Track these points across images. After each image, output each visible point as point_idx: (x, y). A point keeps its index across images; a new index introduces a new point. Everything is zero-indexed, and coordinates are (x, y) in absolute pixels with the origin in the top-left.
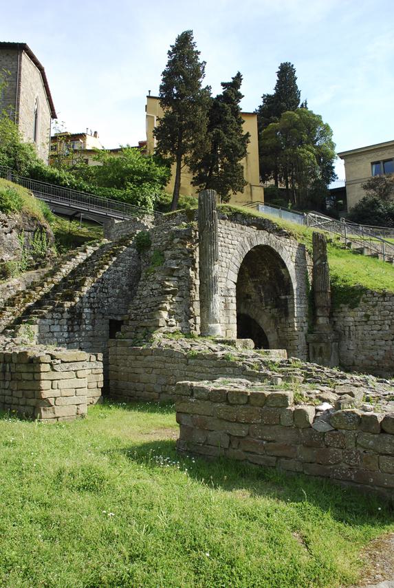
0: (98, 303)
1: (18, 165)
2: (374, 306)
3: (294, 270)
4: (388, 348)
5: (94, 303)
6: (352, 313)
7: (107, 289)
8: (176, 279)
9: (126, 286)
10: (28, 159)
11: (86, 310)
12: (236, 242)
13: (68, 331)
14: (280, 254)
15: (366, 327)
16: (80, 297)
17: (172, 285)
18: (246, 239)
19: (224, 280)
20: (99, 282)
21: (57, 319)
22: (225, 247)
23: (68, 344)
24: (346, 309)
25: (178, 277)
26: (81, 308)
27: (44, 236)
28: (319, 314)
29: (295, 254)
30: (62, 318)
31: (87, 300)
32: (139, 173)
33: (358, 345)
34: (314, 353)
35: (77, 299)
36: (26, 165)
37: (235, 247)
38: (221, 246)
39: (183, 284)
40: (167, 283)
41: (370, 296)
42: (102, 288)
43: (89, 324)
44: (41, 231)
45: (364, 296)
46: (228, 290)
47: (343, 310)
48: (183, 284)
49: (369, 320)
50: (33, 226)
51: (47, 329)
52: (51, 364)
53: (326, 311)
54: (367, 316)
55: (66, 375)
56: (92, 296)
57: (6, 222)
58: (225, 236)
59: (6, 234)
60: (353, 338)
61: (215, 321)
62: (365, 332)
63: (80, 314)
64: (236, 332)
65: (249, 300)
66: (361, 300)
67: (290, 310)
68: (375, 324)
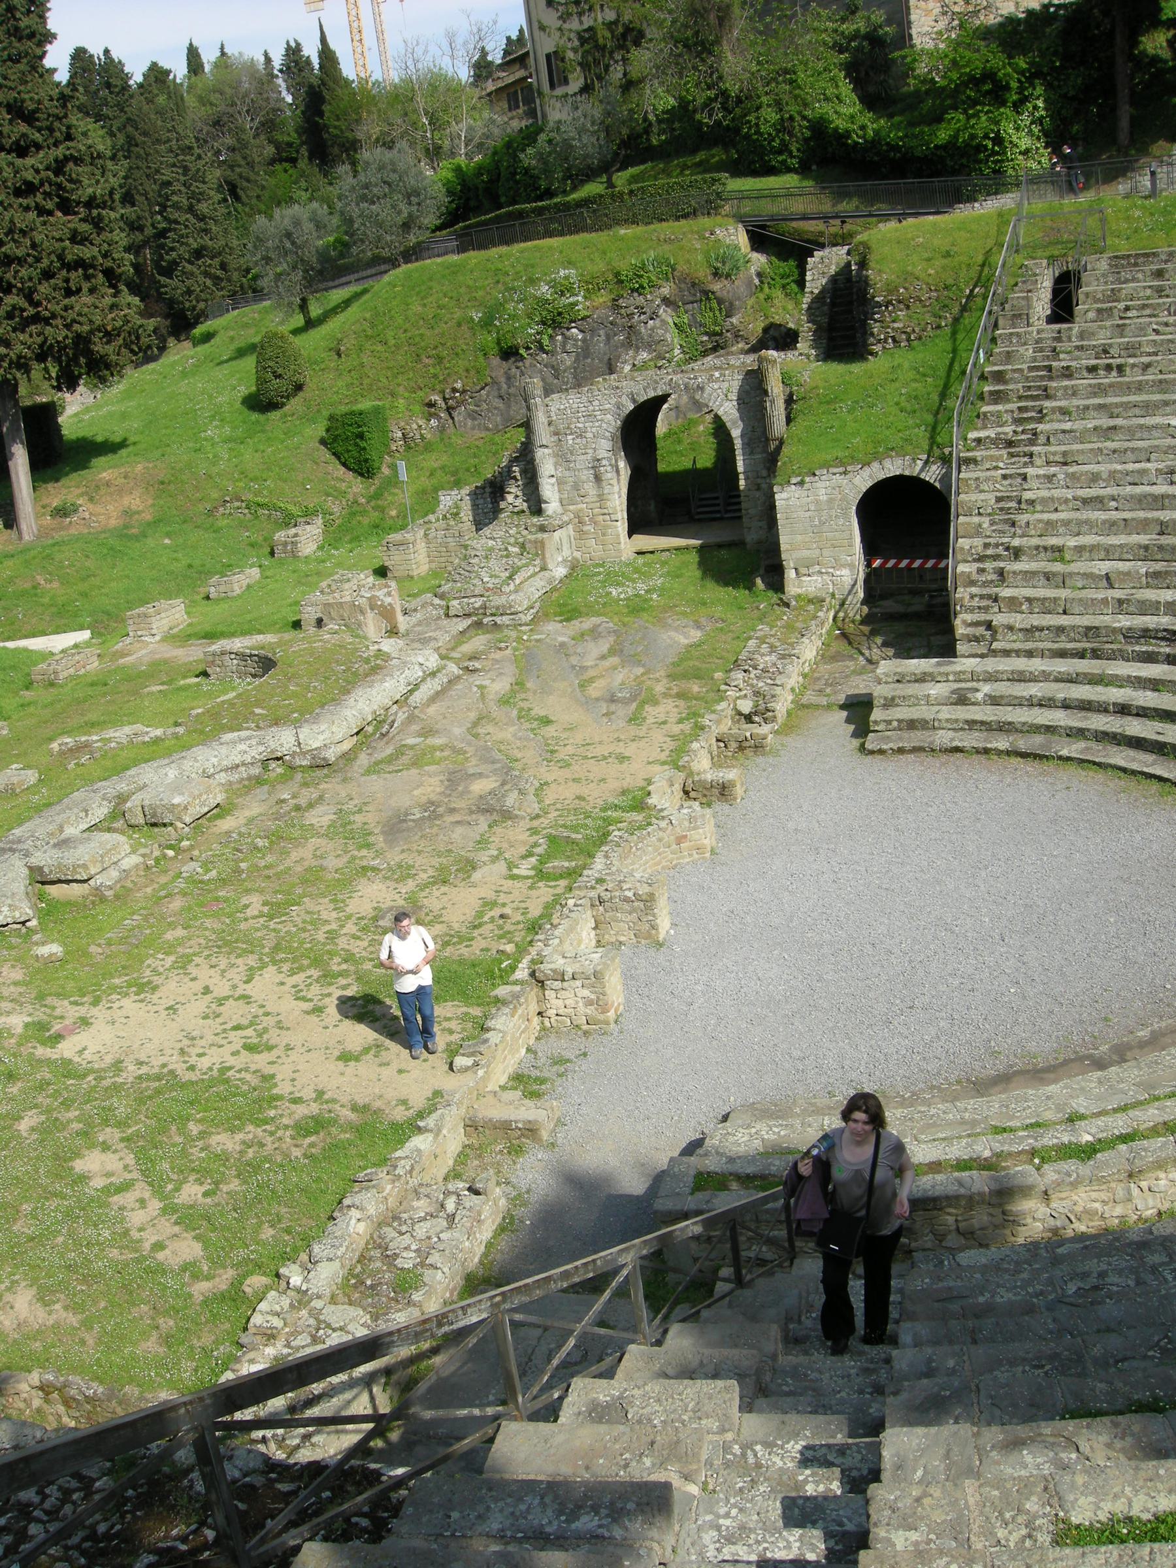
10: (806, 105)
27: (715, 305)
36: (804, 118)
44: (708, 299)
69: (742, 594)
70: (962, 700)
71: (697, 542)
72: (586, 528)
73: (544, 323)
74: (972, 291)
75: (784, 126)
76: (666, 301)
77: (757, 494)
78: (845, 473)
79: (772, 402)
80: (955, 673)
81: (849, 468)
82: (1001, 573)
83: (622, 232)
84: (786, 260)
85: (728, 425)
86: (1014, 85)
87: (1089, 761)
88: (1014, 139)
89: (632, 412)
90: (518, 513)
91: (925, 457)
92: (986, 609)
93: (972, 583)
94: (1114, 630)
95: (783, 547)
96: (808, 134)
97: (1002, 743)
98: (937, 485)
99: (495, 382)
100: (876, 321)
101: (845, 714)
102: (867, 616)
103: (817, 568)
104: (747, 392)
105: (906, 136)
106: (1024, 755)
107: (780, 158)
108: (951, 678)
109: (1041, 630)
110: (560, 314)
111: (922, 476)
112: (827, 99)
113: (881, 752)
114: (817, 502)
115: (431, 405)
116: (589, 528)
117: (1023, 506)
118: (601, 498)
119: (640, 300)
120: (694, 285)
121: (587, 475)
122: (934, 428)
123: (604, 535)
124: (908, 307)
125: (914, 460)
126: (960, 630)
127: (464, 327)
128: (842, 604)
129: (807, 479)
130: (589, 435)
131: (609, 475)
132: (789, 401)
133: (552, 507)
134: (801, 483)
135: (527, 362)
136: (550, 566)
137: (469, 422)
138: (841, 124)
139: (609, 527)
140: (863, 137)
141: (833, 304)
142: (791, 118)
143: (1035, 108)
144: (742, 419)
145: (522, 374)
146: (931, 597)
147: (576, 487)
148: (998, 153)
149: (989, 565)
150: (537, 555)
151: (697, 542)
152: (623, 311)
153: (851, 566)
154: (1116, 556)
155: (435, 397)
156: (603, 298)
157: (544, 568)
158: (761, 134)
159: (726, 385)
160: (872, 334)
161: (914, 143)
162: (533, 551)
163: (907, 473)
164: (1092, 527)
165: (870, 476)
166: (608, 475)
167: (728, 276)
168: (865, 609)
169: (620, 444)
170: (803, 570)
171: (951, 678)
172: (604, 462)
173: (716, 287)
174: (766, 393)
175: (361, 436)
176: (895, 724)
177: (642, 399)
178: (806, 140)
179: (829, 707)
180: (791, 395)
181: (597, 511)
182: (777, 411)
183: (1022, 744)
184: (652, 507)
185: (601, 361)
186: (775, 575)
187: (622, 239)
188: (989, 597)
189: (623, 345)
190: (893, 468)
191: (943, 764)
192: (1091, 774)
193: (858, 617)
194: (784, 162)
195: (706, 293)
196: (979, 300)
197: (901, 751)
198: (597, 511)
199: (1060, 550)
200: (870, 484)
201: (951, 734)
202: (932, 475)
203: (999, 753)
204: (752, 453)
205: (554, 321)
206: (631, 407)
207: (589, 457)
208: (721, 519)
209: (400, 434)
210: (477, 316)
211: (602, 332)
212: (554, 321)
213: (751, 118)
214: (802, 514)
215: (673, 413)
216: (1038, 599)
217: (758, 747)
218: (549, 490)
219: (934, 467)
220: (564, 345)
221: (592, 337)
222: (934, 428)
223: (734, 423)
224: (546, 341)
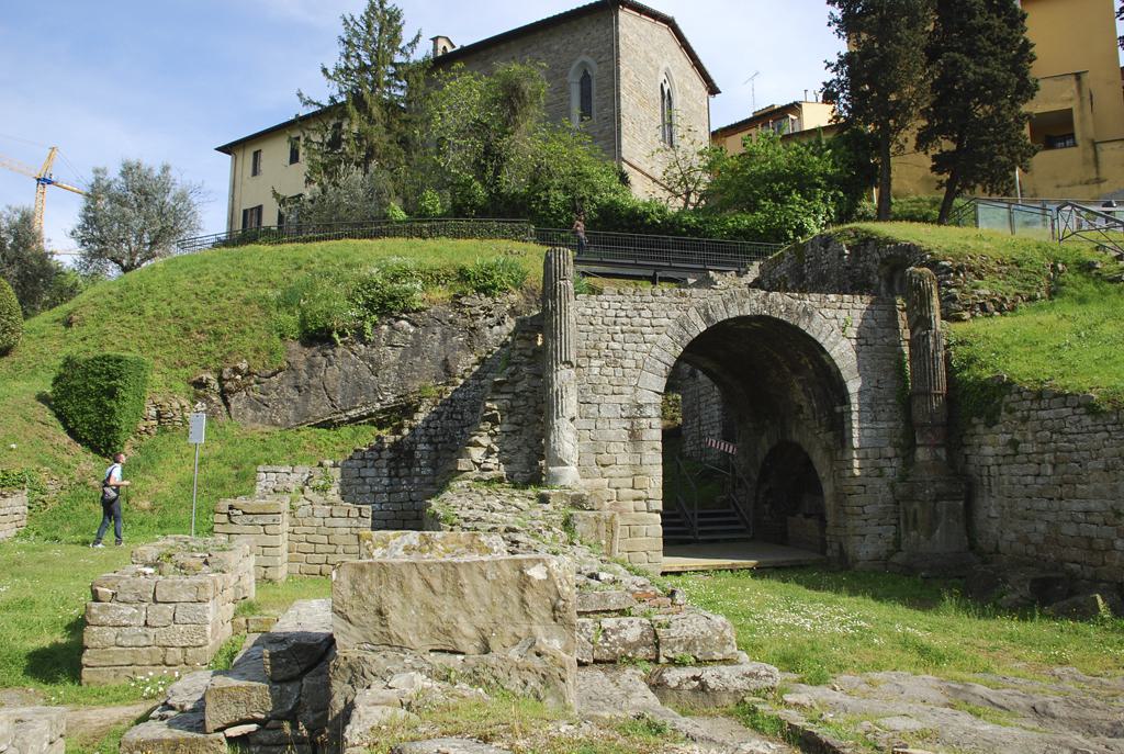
0: (444, 435)
1: (577, 204)
2: (1025, 420)
3: (853, 355)
4: (1051, 517)
5: (436, 435)
6: (989, 438)
7: (462, 413)
8: (509, 396)
10: (595, 191)
11: (421, 447)
12: (665, 321)
13: (390, 476)
14: (803, 326)
15: (1015, 469)
16: (410, 428)
17: (496, 407)
18: (692, 312)
19: (629, 390)
20: (447, 405)
21: (371, 460)
22: (633, 332)
23: (389, 494)
24: (981, 429)
25: (515, 393)
26: (411, 443)
28: (918, 442)
29: (857, 322)
30: (380, 458)
31: (422, 432)
32: (777, 176)
33: (1003, 507)
34: (906, 522)
35: (406, 431)
36: (593, 201)
37: (661, 330)
38: (623, 332)
39: (522, 403)
40: (488, 404)
41: (1017, 397)
42: (452, 413)
43: (426, 466)
45: (1007, 398)
46: (640, 406)
47: (977, 430)
48: (522, 403)
49: (1017, 454)
51: (354, 473)
52: (228, 514)
53: (930, 435)
54: (1014, 444)
55: (249, 529)
56: (432, 425)
57: (490, 310)
58: (630, 313)
59: (491, 327)
60: (994, 490)
61: (562, 463)
62: (1014, 479)
63: (411, 453)
64: (659, 481)
65: (801, 416)
66: (1003, 408)
67: (847, 435)
68: (1030, 462)
71: (751, 563)
75: (574, 206)
77: (879, 482)
85: (845, 374)
90: (489, 482)
99: (292, 368)
110: (393, 298)
115: (200, 384)
119: (487, 301)
121: (618, 430)
130: (629, 363)
135: (339, 351)
137: (250, 413)
145: (330, 363)
151: (751, 563)
152: (466, 310)
155: (206, 376)
156: (440, 293)
158: (549, 211)
159: (843, 314)
162: (590, 538)
172: (649, 411)
175: (111, 393)
177: (720, 316)
181: (625, 492)
185: (433, 361)
189: (462, 347)
204: (875, 420)
205: (383, 306)
206: (703, 328)
207: (624, 399)
208: (697, 542)
209: (153, 412)
211: (438, 330)
212: (383, 306)
220: (390, 336)
221: (425, 332)
224: (368, 326)
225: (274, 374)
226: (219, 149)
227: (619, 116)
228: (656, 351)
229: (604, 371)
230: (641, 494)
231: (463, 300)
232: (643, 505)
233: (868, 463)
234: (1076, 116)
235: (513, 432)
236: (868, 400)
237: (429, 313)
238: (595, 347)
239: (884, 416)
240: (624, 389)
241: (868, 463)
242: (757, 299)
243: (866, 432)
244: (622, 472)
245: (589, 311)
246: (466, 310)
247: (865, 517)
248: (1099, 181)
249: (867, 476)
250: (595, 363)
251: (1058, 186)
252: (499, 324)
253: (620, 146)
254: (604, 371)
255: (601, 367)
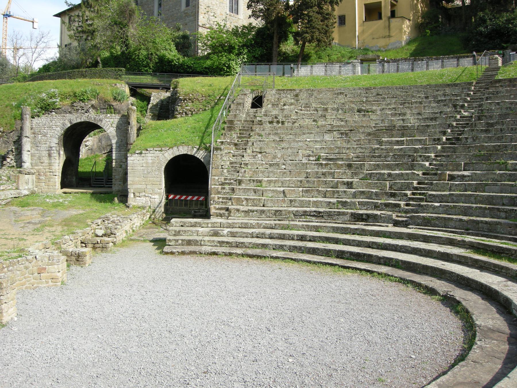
9: (200, 132)
10: (158, 50)
12: (58, 124)
36: (157, 55)
44: (110, 108)
46: (51, 147)
50: (105, 106)
58: (49, 122)
69: (108, 205)
70: (216, 234)
71: (91, 191)
72: (41, 177)
73: (41, 108)
74: (220, 98)
75: (149, 57)
76: (93, 106)
77: (120, 169)
78: (161, 151)
79: (131, 128)
80: (212, 223)
81: (163, 149)
82: (233, 190)
83: (80, 80)
84: (143, 102)
85: (111, 137)
86: (237, 47)
87: (289, 258)
88: (235, 67)
89: (69, 128)
91: (198, 147)
92: (226, 203)
93: (219, 193)
94: (289, 212)
95: (129, 182)
96: (157, 61)
97: (239, 251)
98: (202, 160)
100: (179, 106)
101: (153, 244)
102: (165, 218)
103: (144, 194)
104: (121, 124)
105: (194, 63)
106: (251, 256)
107: (145, 69)
108: (210, 225)
109: (253, 211)
110: (49, 105)
111: (196, 155)
112: (166, 50)
113: (172, 253)
114: (147, 163)
116: (42, 177)
117: (242, 166)
118: (50, 164)
119: (82, 104)
120: (105, 102)
121: (45, 153)
122: (203, 137)
123: (49, 181)
124: (193, 102)
125: (193, 148)
126: (213, 211)
127: (9, 108)
128: (154, 212)
129: (143, 152)
130: (49, 136)
131: (55, 155)
132: (139, 129)
133: (27, 165)
134: (141, 153)
136: (20, 188)
137: (3, 145)
138: (171, 57)
139: (52, 178)
140: (178, 63)
141: (161, 109)
142: (152, 54)
143: (244, 58)
144: (117, 136)
146: (195, 212)
147: (39, 158)
148: (228, 72)
149: (227, 187)
150: (15, 182)
151: (91, 191)
152: (75, 108)
153: (159, 194)
154: (287, 185)
156: (68, 102)
157: (17, 189)
158: (139, 59)
159: (112, 120)
160: (177, 111)
161: (197, 66)
162: (13, 180)
163: (189, 153)
164: (274, 174)
165: (172, 153)
166: (55, 154)
167: (119, 101)
168: (164, 215)
169: (62, 143)
170: (137, 194)
171: (210, 225)
172: (54, 148)
173: (114, 104)
174: (129, 123)
176: (180, 242)
177: (75, 122)
178: (156, 63)
179: (145, 241)
180: (140, 127)
182: (133, 131)
183: (250, 251)
184: (74, 179)
186: (124, 197)
187: (79, 82)
188: (227, 198)
190: (183, 150)
191: (206, 259)
192: (291, 264)
193: (161, 218)
194: (147, 71)
195: (110, 106)
196: (222, 101)
197: (183, 253)
198: (47, 170)
199: (260, 181)
200: (172, 157)
201: (210, 247)
202: (200, 155)
203: (238, 255)
204: (120, 151)
206: (69, 125)
207: (47, 145)
210: (14, 104)
212: (46, 108)
213: (137, 52)
214: (139, 168)
215: (90, 151)
216: (251, 199)
217: (104, 248)
218: (26, 157)
219: (201, 152)
222: (203, 137)
223: (114, 137)
225: (11, 132)
226: (54, 16)
227: (198, 5)
228: (56, 132)
229: (42, 138)
230: (51, 171)
231: (74, 104)
232: (52, 174)
233: (117, 163)
234: (383, 5)
235: (18, 154)
236: (118, 145)
237: (62, 109)
238: (40, 132)
239: (123, 150)
240: (47, 143)
241: (117, 163)
242: (85, 117)
243: (117, 154)
244: (46, 165)
245: (38, 122)
246: (75, 108)
247: (115, 179)
248: (389, 36)
249: (117, 167)
250: (40, 136)
251: (373, 39)
252: (86, 112)
253: (198, 19)
254: (42, 138)
255: (41, 137)
